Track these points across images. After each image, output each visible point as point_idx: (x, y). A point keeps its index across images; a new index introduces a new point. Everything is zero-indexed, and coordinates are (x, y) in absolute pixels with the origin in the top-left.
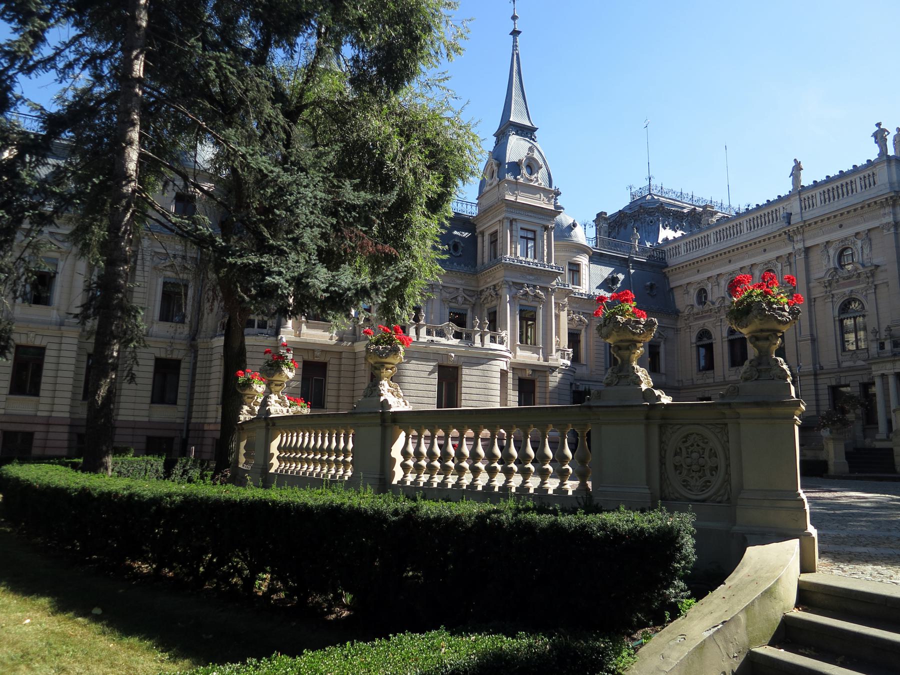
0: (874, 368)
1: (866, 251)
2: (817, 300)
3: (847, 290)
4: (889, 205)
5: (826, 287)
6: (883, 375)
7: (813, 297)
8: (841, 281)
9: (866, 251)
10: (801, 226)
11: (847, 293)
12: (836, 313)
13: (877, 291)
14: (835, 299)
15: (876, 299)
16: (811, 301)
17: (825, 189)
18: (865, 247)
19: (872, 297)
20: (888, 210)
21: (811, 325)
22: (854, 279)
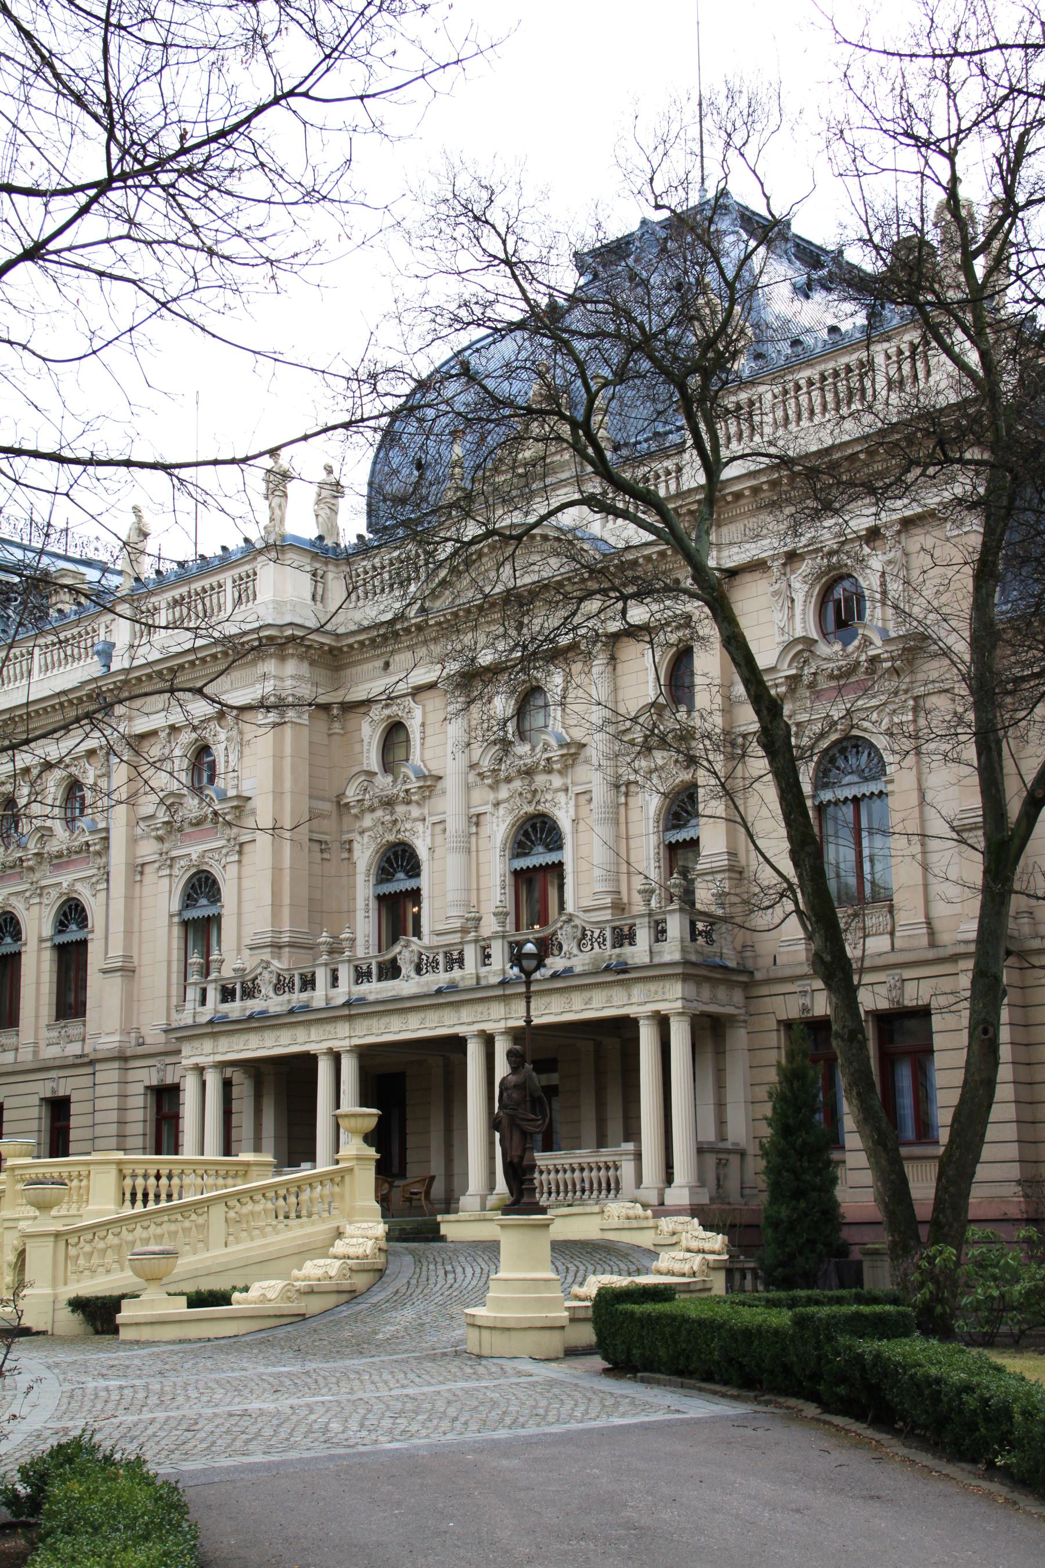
0: (186, 1049)
1: (233, 758)
2: (148, 869)
3: (195, 851)
4: (271, 656)
5: (160, 839)
6: (200, 1070)
7: (140, 861)
8: (188, 830)
9: (233, 758)
10: (125, 682)
11: (194, 857)
12: (176, 906)
13: (246, 859)
14: (176, 871)
15: (239, 878)
16: (138, 869)
17: (176, 593)
18: (230, 750)
19: (232, 870)
20: (270, 666)
21: (128, 932)
22: (208, 825)
